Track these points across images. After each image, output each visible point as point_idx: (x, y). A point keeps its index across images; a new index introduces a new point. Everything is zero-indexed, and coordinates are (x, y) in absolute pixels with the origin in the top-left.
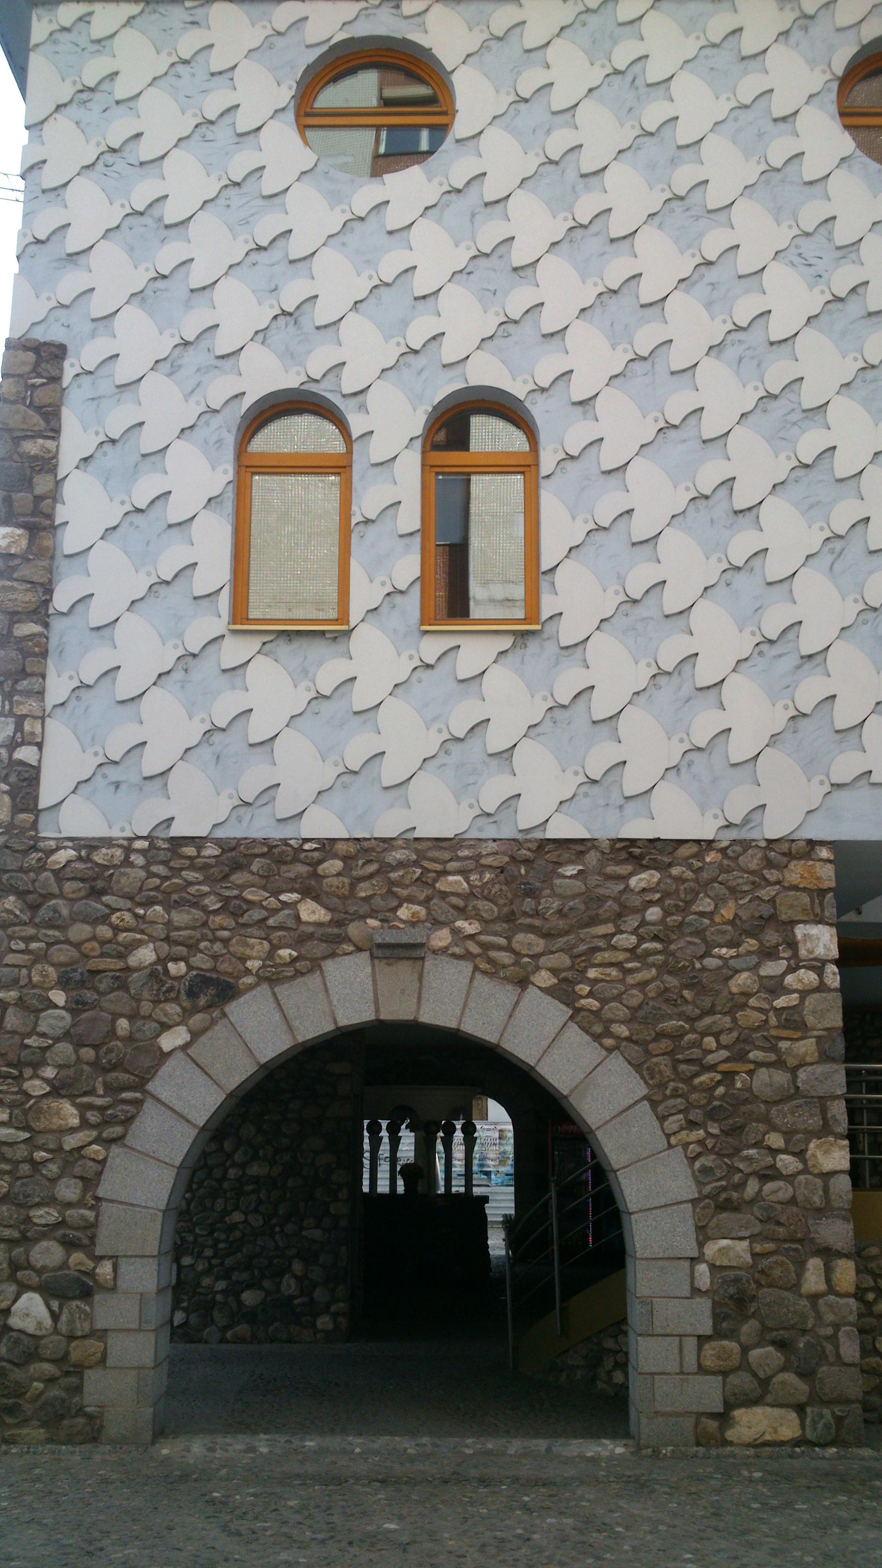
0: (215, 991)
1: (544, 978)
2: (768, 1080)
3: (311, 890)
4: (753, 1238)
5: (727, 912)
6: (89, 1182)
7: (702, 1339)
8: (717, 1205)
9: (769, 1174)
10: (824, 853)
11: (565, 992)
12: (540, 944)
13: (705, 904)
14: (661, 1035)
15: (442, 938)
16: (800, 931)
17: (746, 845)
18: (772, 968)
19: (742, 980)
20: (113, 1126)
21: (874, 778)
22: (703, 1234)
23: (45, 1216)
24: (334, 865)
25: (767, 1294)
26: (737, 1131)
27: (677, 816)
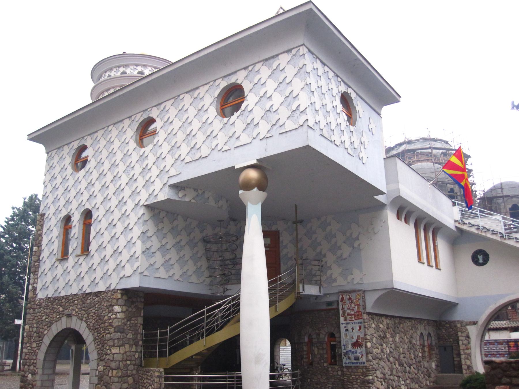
0: (50, 324)
1: (84, 319)
2: (108, 336)
3: (61, 306)
4: (104, 366)
5: (105, 305)
6: (36, 356)
7: (96, 384)
8: (100, 359)
9: (107, 354)
10: (118, 291)
11: (86, 322)
12: (84, 313)
13: (103, 304)
14: (96, 329)
15: (74, 313)
16: (115, 307)
17: (109, 291)
18: (110, 315)
19: (106, 318)
20: (39, 347)
21: (126, 276)
22: (98, 365)
23: (32, 361)
24: (64, 300)
25: (105, 377)
26: (103, 346)
27: (101, 287)
